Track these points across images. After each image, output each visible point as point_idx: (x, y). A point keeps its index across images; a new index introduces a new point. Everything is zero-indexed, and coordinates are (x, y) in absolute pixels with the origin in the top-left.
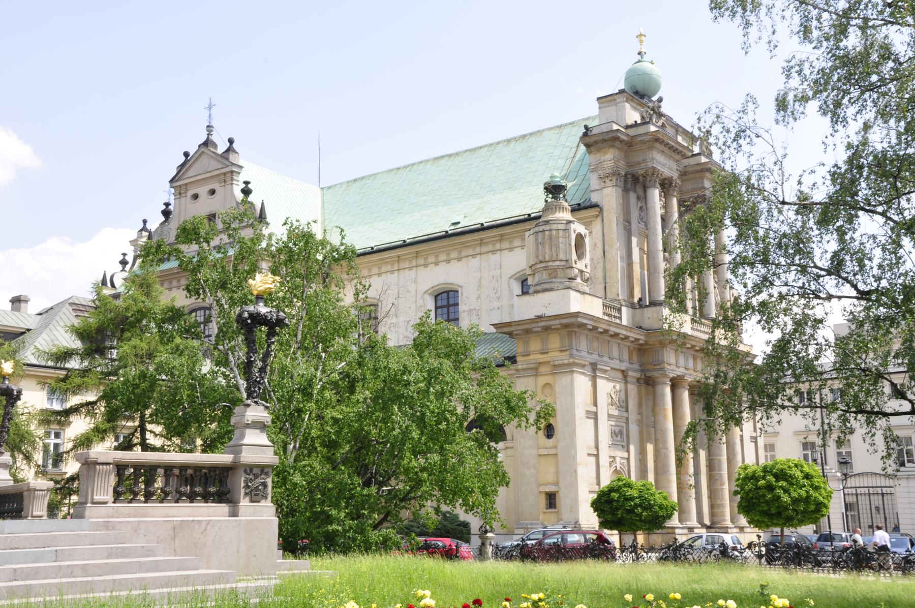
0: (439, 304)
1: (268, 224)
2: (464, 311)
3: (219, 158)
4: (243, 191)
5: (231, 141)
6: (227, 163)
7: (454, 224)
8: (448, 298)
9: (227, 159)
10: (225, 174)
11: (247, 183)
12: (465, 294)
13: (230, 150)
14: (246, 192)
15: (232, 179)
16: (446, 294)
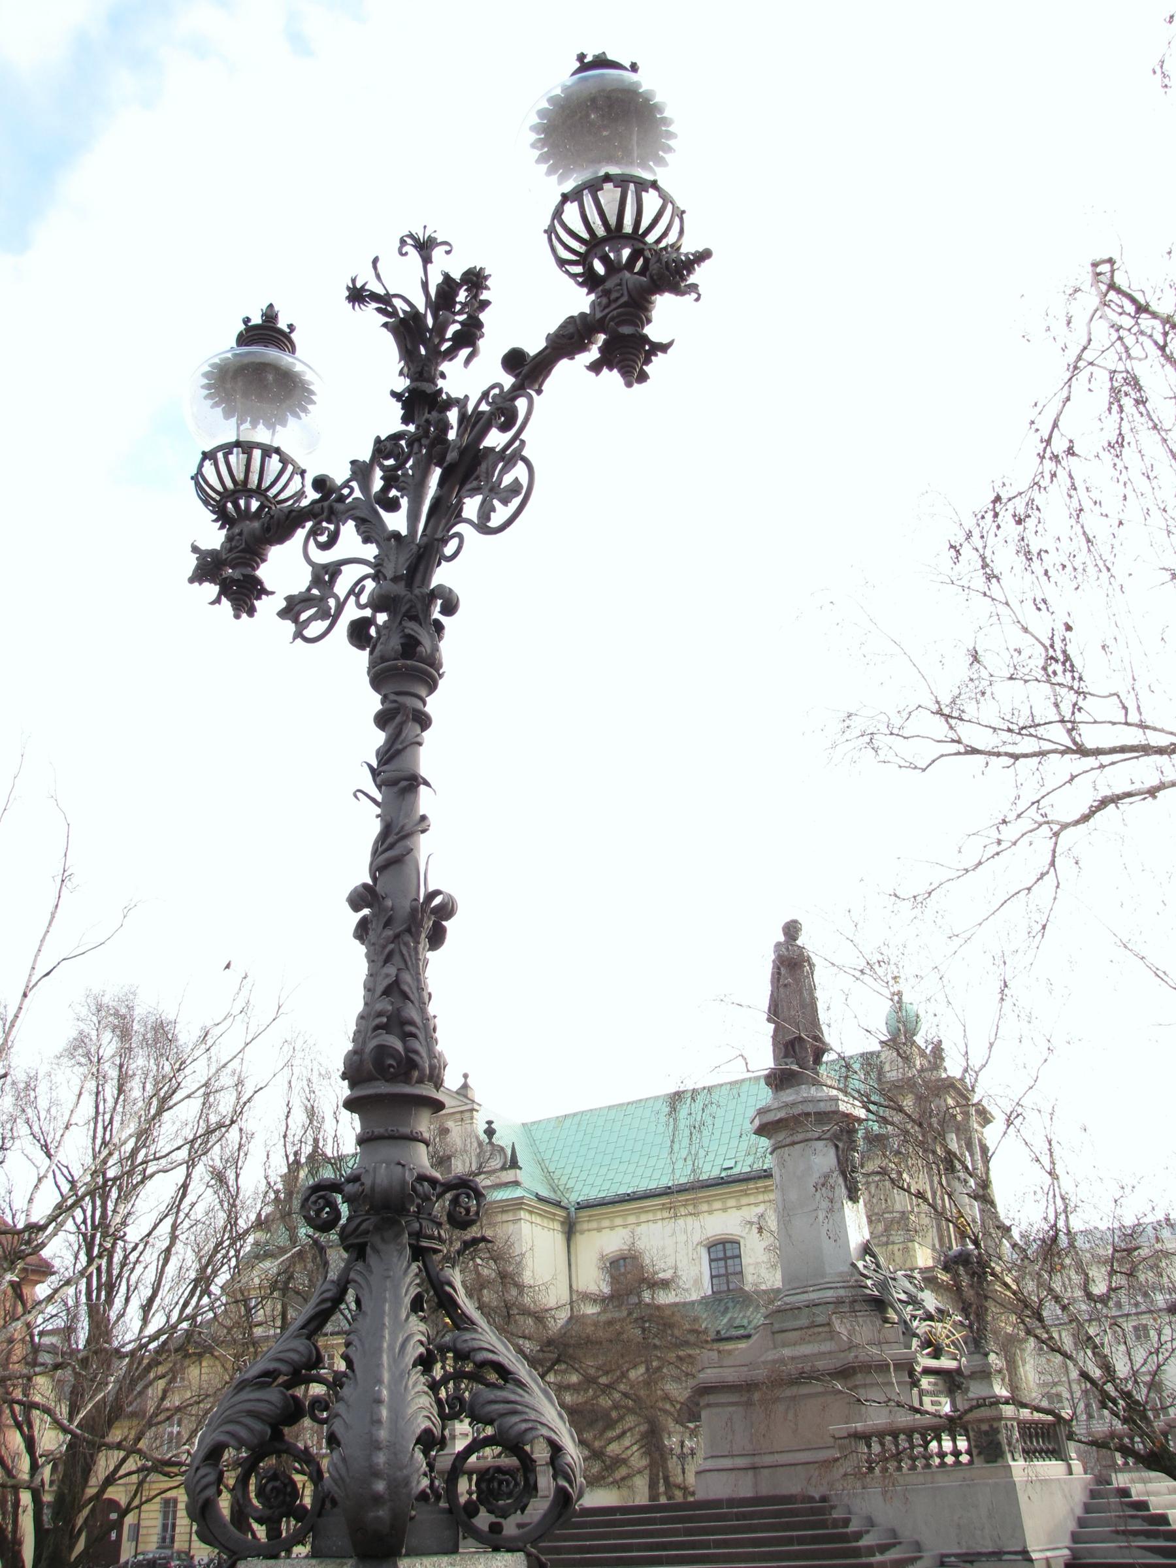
0: (737, 1261)
1: (520, 1168)
2: (749, 1264)
3: (455, 1095)
4: (485, 1132)
5: (466, 1076)
6: (465, 1100)
7: (725, 1169)
8: (725, 1250)
9: (466, 1097)
10: (462, 1112)
11: (490, 1123)
12: (748, 1246)
13: (465, 1086)
14: (490, 1132)
15: (472, 1118)
16: (720, 1247)
